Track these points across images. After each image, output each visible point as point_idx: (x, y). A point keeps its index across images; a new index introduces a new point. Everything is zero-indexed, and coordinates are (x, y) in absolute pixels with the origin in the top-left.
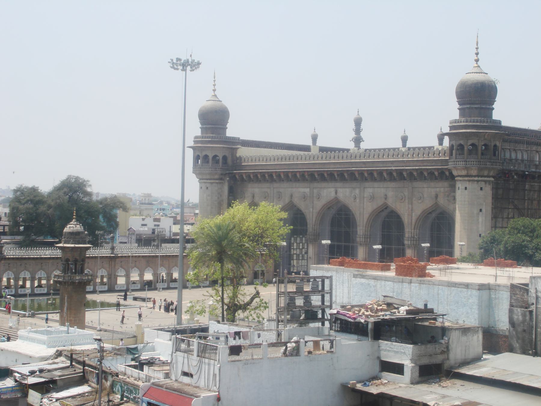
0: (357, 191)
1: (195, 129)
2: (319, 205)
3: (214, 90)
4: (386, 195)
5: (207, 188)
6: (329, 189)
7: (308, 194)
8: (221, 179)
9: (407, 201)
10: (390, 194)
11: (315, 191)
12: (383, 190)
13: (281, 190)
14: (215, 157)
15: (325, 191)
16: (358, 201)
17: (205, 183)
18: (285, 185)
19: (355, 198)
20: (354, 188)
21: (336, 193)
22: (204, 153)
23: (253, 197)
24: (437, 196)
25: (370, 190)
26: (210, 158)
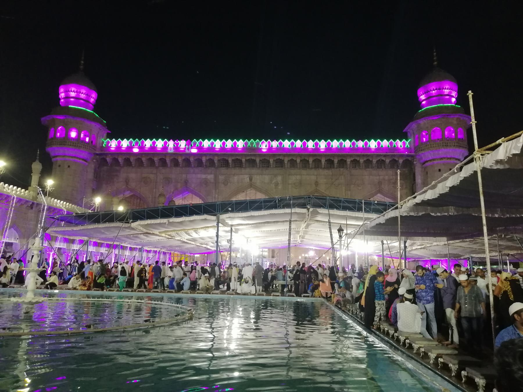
0: (279, 178)
4: (317, 182)
5: (69, 166)
6: (241, 176)
7: (212, 181)
9: (344, 188)
10: (322, 181)
12: (313, 178)
15: (236, 178)
16: (280, 187)
18: (178, 169)
19: (277, 184)
20: (276, 175)
21: (251, 179)
24: (380, 183)
25: (298, 177)
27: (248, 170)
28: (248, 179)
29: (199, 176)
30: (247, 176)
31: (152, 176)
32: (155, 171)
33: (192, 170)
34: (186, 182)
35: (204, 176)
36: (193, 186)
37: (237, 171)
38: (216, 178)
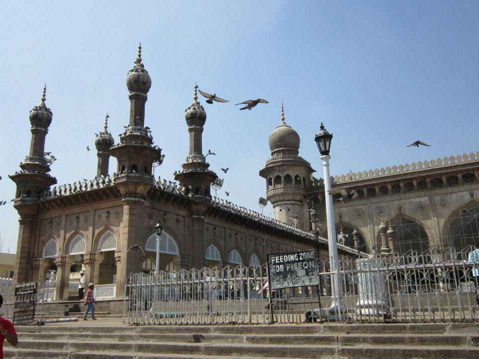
1: (265, 157)
2: (446, 212)
3: (283, 119)
6: (460, 194)
7: (428, 202)
8: (301, 201)
11: (437, 198)
13: (382, 204)
14: (297, 176)
15: (453, 196)
17: (286, 204)
18: (388, 198)
21: (472, 195)
22: (285, 174)
23: (341, 217)
26: (293, 177)
27: (466, 187)
28: (469, 195)
29: (412, 200)
30: (467, 192)
31: (363, 207)
32: (365, 201)
33: (403, 196)
34: (400, 208)
35: (417, 200)
36: (407, 211)
37: (455, 189)
38: (430, 198)
